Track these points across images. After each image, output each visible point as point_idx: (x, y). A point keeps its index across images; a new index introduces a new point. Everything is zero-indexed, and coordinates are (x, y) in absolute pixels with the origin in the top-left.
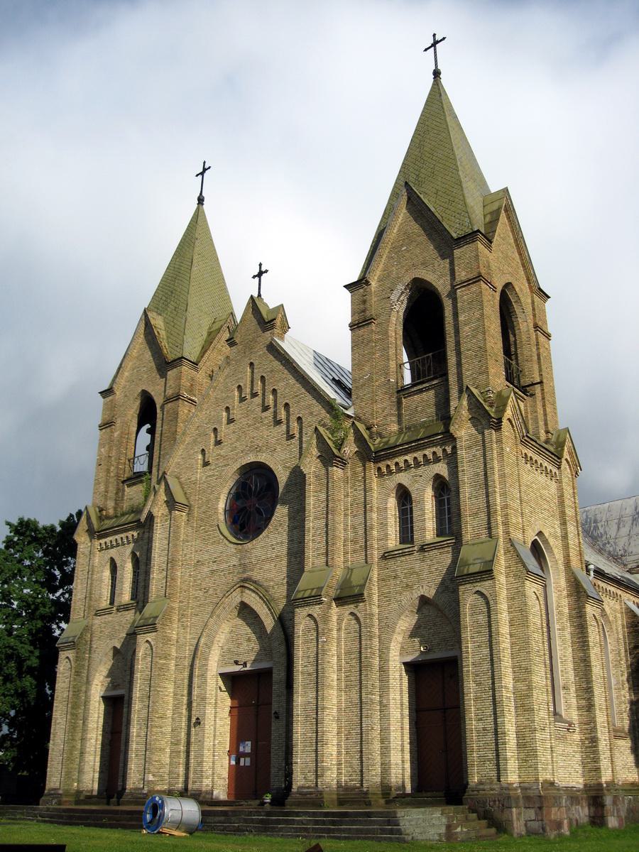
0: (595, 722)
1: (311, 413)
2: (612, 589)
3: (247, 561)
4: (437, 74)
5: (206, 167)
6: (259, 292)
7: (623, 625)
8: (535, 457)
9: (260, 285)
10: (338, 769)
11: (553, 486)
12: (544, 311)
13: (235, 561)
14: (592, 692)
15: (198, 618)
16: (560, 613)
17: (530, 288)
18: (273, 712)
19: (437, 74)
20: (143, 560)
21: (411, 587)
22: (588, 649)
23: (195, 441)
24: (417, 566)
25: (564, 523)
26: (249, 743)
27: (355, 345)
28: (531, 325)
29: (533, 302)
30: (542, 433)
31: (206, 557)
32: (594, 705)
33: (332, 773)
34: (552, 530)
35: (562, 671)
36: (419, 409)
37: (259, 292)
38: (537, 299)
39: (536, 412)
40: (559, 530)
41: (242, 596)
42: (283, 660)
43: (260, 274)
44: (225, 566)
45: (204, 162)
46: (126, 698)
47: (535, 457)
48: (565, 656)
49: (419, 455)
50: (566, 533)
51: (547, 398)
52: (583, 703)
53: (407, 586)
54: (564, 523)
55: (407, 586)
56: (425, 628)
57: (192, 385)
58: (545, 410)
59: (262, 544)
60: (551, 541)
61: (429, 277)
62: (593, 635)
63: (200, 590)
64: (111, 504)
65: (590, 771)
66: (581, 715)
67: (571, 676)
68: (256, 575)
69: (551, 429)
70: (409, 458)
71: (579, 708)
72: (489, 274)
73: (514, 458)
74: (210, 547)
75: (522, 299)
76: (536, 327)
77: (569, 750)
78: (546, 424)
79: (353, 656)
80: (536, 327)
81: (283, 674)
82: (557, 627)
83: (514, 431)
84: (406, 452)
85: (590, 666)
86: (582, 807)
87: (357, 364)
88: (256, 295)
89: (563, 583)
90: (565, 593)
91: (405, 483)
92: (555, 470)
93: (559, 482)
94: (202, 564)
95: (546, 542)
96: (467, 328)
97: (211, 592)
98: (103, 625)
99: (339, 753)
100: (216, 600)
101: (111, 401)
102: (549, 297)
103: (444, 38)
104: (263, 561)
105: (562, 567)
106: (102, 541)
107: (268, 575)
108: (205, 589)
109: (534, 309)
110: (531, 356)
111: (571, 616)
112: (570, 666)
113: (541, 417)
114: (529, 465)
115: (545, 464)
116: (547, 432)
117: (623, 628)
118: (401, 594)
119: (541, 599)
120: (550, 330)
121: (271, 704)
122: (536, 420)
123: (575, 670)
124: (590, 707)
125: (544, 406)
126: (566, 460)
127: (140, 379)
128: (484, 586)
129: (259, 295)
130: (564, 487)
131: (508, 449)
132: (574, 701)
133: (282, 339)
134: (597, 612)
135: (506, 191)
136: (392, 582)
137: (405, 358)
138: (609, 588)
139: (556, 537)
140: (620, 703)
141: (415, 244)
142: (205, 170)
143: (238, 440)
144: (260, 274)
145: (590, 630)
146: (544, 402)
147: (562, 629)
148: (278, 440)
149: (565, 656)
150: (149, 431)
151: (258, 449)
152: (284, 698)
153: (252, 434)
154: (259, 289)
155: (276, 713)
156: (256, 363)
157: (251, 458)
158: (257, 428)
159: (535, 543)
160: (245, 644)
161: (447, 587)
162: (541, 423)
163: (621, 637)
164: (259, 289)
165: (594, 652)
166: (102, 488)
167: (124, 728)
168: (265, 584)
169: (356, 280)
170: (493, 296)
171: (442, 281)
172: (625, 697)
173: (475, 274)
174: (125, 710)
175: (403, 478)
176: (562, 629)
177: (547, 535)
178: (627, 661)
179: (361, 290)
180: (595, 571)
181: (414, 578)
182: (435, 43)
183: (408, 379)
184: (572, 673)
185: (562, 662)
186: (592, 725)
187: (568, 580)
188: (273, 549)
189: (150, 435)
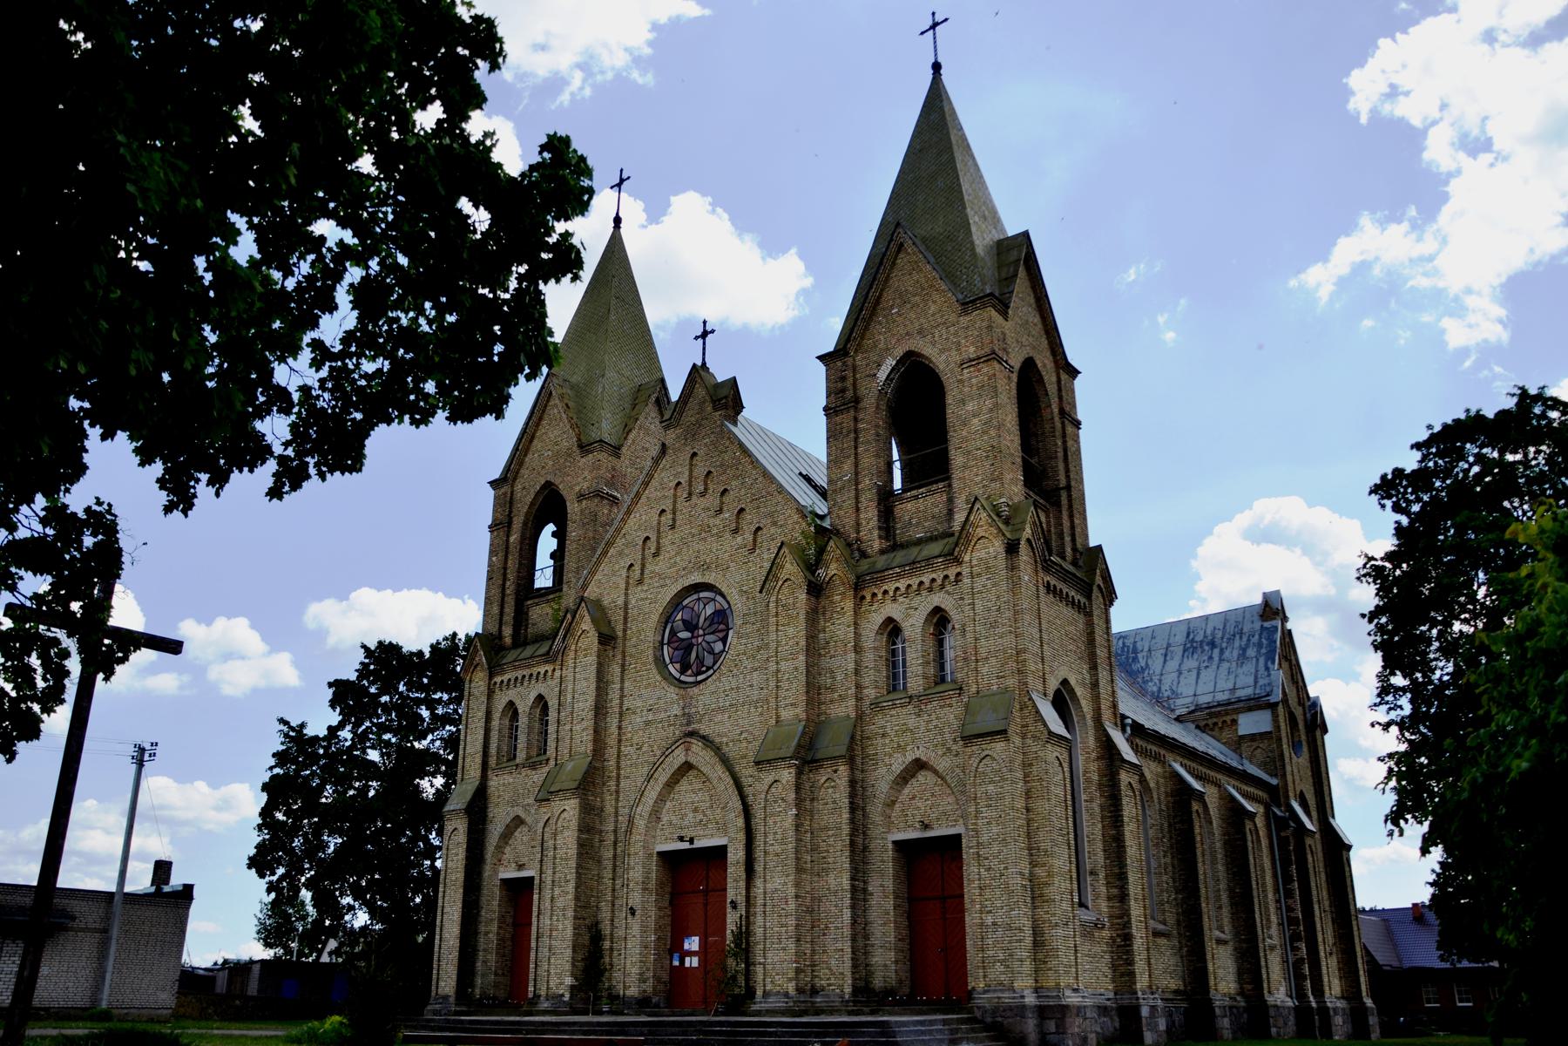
0: (1129, 916)
1: (775, 524)
2: (1154, 748)
3: (693, 710)
4: (937, 67)
5: (624, 176)
6: (704, 359)
7: (1166, 793)
8: (1060, 585)
9: (704, 349)
10: (813, 971)
11: (1081, 620)
12: (1073, 391)
14: (1126, 878)
15: (628, 781)
16: (1088, 780)
17: (1056, 362)
18: (729, 901)
19: (937, 67)
20: (553, 703)
21: (904, 750)
22: (1122, 826)
23: (621, 553)
25: (1094, 667)
26: (696, 939)
27: (832, 435)
28: (1056, 411)
29: (1059, 381)
30: (1068, 550)
32: (1128, 895)
33: (805, 976)
34: (1080, 677)
35: (1089, 852)
36: (914, 521)
37: (704, 359)
38: (1064, 376)
39: (1061, 525)
40: (1087, 677)
41: (687, 755)
42: (742, 836)
43: (705, 334)
44: (663, 715)
45: (622, 170)
46: (537, 882)
47: (1060, 585)
48: (1093, 834)
49: (914, 582)
50: (1097, 680)
51: (1075, 506)
52: (1115, 891)
53: (899, 746)
54: (1094, 667)
55: (899, 746)
56: (921, 798)
57: (613, 476)
58: (1072, 522)
59: (713, 688)
60: (1079, 691)
61: (928, 351)
62: (1129, 809)
63: (632, 745)
64: (508, 632)
65: (1122, 975)
66: (1112, 907)
67: (1100, 858)
68: (704, 729)
69: (1079, 546)
70: (902, 584)
71: (1109, 899)
72: (1005, 349)
73: (1034, 589)
74: (643, 691)
75: (1046, 378)
76: (1062, 412)
77: (1097, 949)
78: (1073, 540)
79: (830, 833)
80: (1062, 412)
81: (741, 854)
82: (1084, 797)
83: (1034, 553)
84: (899, 576)
85: (1124, 847)
86: (1112, 1019)
87: (834, 461)
88: (699, 363)
89: (1091, 742)
90: (1094, 755)
92: (1083, 600)
93: (1089, 615)
94: (634, 713)
95: (1072, 691)
96: (976, 421)
97: (644, 749)
98: (501, 788)
99: (813, 951)
100: (652, 759)
101: (505, 494)
102: (1079, 373)
103: (946, 20)
104: (713, 710)
105: (1090, 722)
106: (498, 679)
107: (722, 729)
108: (637, 744)
109: (1060, 390)
110: (1056, 452)
111: (1100, 785)
112: (1099, 846)
113: (1066, 530)
114: (1051, 596)
115: (1072, 593)
116: (1074, 549)
117: (1167, 796)
118: (891, 756)
119: (1066, 766)
120: (1080, 416)
121: (725, 890)
122: (1061, 536)
123: (1105, 851)
124: (1123, 897)
125: (1071, 517)
126: (1099, 586)
127: (543, 467)
128: (999, 747)
129: (704, 364)
130: (1096, 622)
131: (1026, 578)
132: (1103, 889)
133: (735, 423)
134: (1134, 780)
135: (1026, 235)
136: (880, 741)
137: (896, 456)
138: (1149, 747)
139: (1083, 685)
140: (1162, 891)
141: (909, 306)
142: (622, 181)
143: (677, 554)
144: (705, 334)
145: (1125, 801)
146: (1072, 511)
147: (1091, 800)
149: (1093, 834)
150: (554, 534)
151: (705, 567)
152: (742, 884)
153: (696, 547)
154: (704, 354)
155: (732, 902)
156: (701, 453)
157: (696, 578)
158: (704, 539)
159: (1058, 693)
160: (691, 815)
161: (948, 749)
162: (1068, 539)
163: (1163, 807)
164: (704, 354)
165: (1130, 829)
166: (496, 609)
167: (534, 919)
168: (717, 740)
169: (832, 349)
170: (1009, 378)
171: (944, 357)
172: (1167, 884)
173: (987, 350)
174: (536, 897)
175: (893, 610)
176: (1091, 800)
177: (1073, 682)
178: (1171, 838)
179: (839, 364)
180: (1131, 726)
181: (908, 737)
182: (934, 26)
183: (897, 484)
184: (1101, 854)
185: (1089, 841)
186: (1126, 919)
187: (1097, 739)
188: (727, 696)
189: (556, 540)
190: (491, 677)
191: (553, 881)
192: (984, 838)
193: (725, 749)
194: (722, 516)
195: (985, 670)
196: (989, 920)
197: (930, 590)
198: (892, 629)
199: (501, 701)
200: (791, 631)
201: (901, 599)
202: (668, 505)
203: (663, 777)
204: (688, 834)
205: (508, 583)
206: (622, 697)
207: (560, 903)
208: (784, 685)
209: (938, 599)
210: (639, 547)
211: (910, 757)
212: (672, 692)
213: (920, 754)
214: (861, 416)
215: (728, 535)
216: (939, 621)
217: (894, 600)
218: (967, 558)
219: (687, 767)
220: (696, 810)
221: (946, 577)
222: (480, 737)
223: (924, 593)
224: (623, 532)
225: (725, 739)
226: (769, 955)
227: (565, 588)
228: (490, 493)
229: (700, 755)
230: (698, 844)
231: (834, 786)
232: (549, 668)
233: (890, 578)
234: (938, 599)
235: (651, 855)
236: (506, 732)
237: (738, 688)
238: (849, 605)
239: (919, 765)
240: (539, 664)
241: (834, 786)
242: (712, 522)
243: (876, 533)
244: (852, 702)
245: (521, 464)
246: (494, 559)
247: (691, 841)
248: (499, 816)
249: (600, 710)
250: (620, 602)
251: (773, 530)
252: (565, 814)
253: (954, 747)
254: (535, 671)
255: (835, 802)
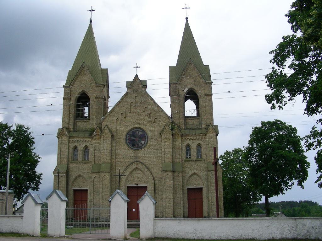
13: (132, 155)
24: (193, 166)
31: (121, 152)
44: (128, 156)
49: (195, 137)
53: (190, 169)
55: (190, 169)
64: (71, 128)
68: (141, 160)
70: (192, 137)
91: (190, 143)
97: (123, 163)
101: (68, 90)
148: (147, 123)
151: (140, 124)
157: (137, 126)
166: (67, 121)
168: (145, 163)
175: (190, 143)
190: (69, 138)
191: (102, 192)
192: (212, 189)
193: (147, 166)
194: (144, 113)
195: (210, 157)
196: (213, 204)
197: (198, 140)
198: (188, 146)
199: (72, 145)
200: (167, 143)
201: (191, 140)
202: (129, 107)
203: (130, 170)
204: (137, 183)
205: (70, 115)
206: (116, 150)
207: (104, 197)
208: (166, 154)
209: (199, 142)
210: (120, 115)
211: (193, 172)
212: (131, 151)
213: (196, 172)
214: (180, 99)
215: (146, 118)
216: (199, 145)
217: (190, 140)
218: (207, 135)
219: (137, 168)
220: (138, 178)
221: (202, 138)
222: (66, 154)
223: (197, 140)
224: (115, 110)
225: (147, 163)
226: (166, 209)
227: (91, 120)
228: (63, 89)
229: (140, 166)
230: (139, 185)
231: (179, 177)
232: (90, 140)
233: (190, 136)
234: (199, 142)
235: (125, 187)
236: (73, 153)
237: (150, 153)
238: (180, 139)
239: (195, 174)
240: (86, 138)
241: (179, 177)
242: (141, 113)
243: (183, 125)
244: (181, 160)
245: (74, 83)
246: (65, 107)
247: (137, 185)
248: (73, 175)
249: (111, 152)
250: (115, 127)
251: (160, 119)
252: (105, 176)
253: (203, 171)
254: (85, 139)
255: (178, 180)
